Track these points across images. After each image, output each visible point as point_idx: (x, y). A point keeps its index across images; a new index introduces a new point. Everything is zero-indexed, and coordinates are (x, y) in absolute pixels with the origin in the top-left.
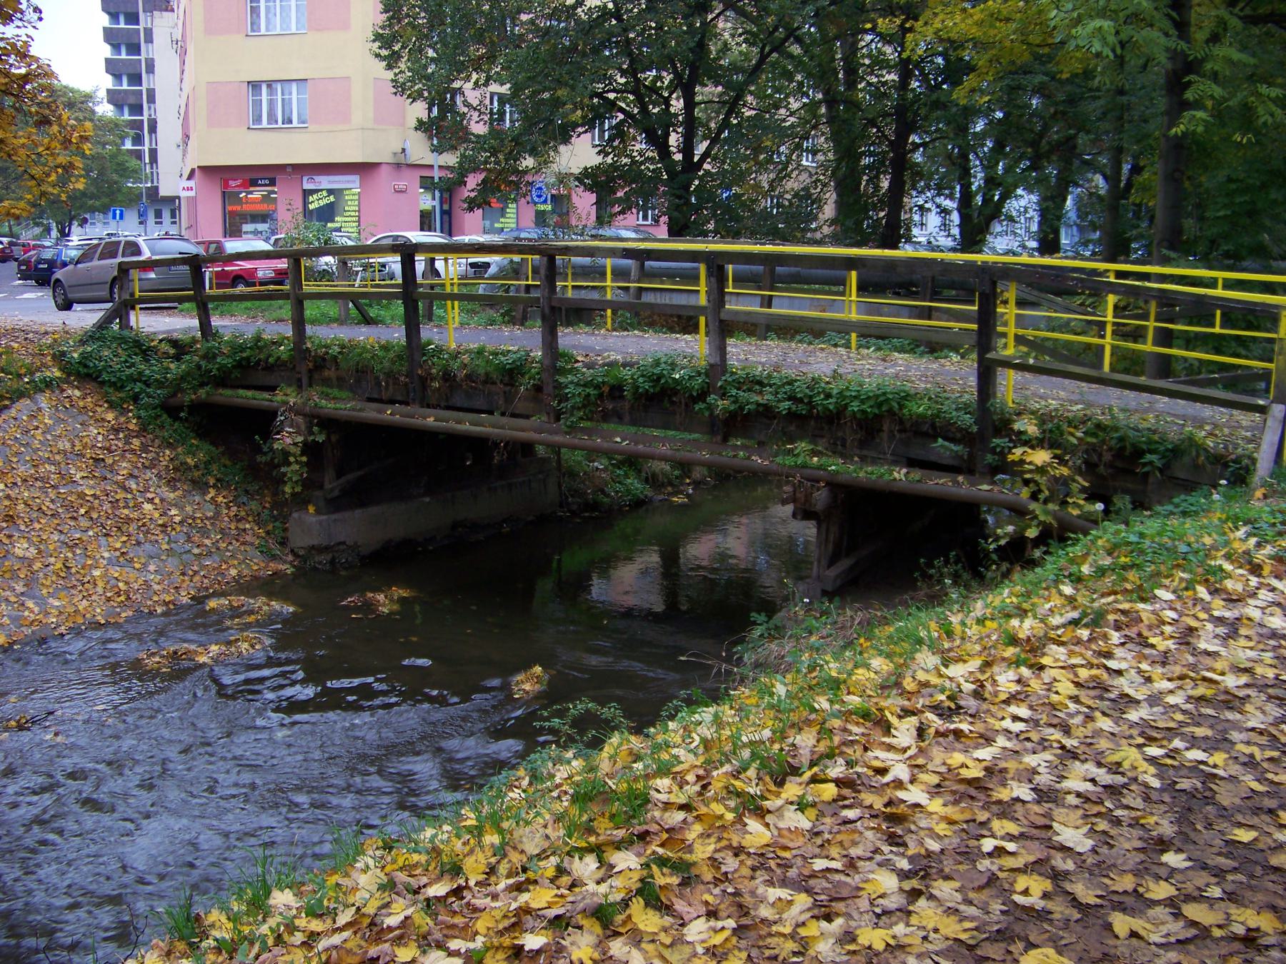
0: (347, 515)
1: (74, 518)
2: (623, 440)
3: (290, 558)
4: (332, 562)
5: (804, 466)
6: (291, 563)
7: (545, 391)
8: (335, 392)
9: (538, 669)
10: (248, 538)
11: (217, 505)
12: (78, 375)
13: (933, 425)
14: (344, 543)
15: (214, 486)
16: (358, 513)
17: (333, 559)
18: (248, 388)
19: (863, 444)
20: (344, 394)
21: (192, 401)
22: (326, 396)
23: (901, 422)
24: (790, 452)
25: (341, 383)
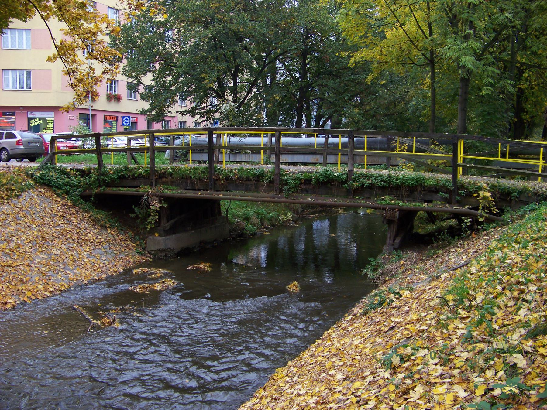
0: (171, 237)
1: (67, 239)
2: (312, 199)
3: (148, 255)
4: (166, 256)
5: (389, 204)
6: (149, 257)
7: (275, 182)
8: (170, 187)
9: (295, 283)
10: (131, 247)
11: (113, 235)
12: (40, 183)
13: (436, 188)
14: (170, 248)
15: (109, 228)
16: (174, 236)
17: (166, 254)
18: (122, 187)
19: (409, 196)
20: (175, 188)
21: (96, 193)
22: (167, 189)
23: (424, 187)
24: (382, 200)
25: (172, 183)
